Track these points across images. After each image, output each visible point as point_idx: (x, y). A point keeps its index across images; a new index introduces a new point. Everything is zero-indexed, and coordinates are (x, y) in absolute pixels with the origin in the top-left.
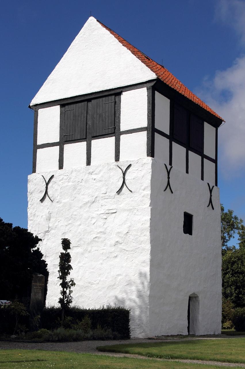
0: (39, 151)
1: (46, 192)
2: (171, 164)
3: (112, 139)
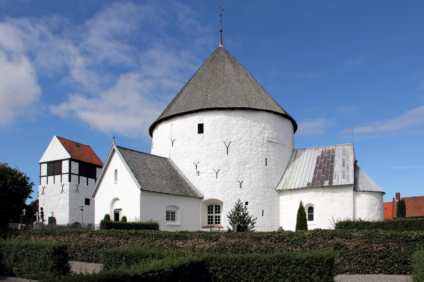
0: (41, 178)
1: (43, 192)
2: (79, 183)
3: (60, 176)
